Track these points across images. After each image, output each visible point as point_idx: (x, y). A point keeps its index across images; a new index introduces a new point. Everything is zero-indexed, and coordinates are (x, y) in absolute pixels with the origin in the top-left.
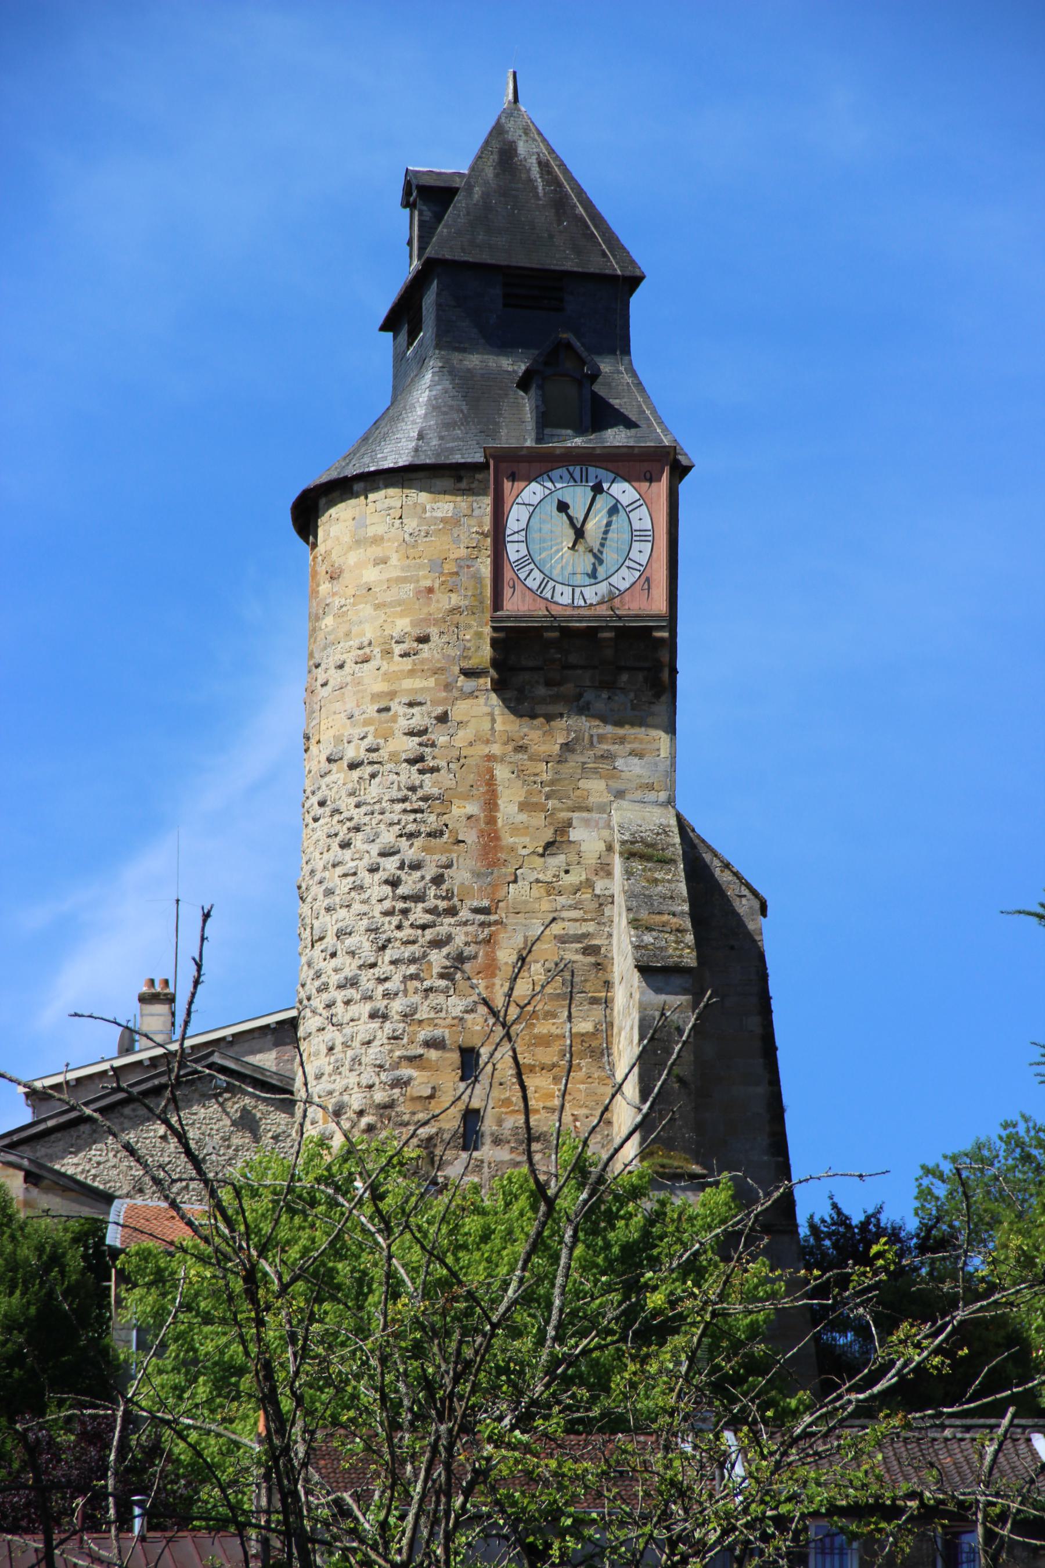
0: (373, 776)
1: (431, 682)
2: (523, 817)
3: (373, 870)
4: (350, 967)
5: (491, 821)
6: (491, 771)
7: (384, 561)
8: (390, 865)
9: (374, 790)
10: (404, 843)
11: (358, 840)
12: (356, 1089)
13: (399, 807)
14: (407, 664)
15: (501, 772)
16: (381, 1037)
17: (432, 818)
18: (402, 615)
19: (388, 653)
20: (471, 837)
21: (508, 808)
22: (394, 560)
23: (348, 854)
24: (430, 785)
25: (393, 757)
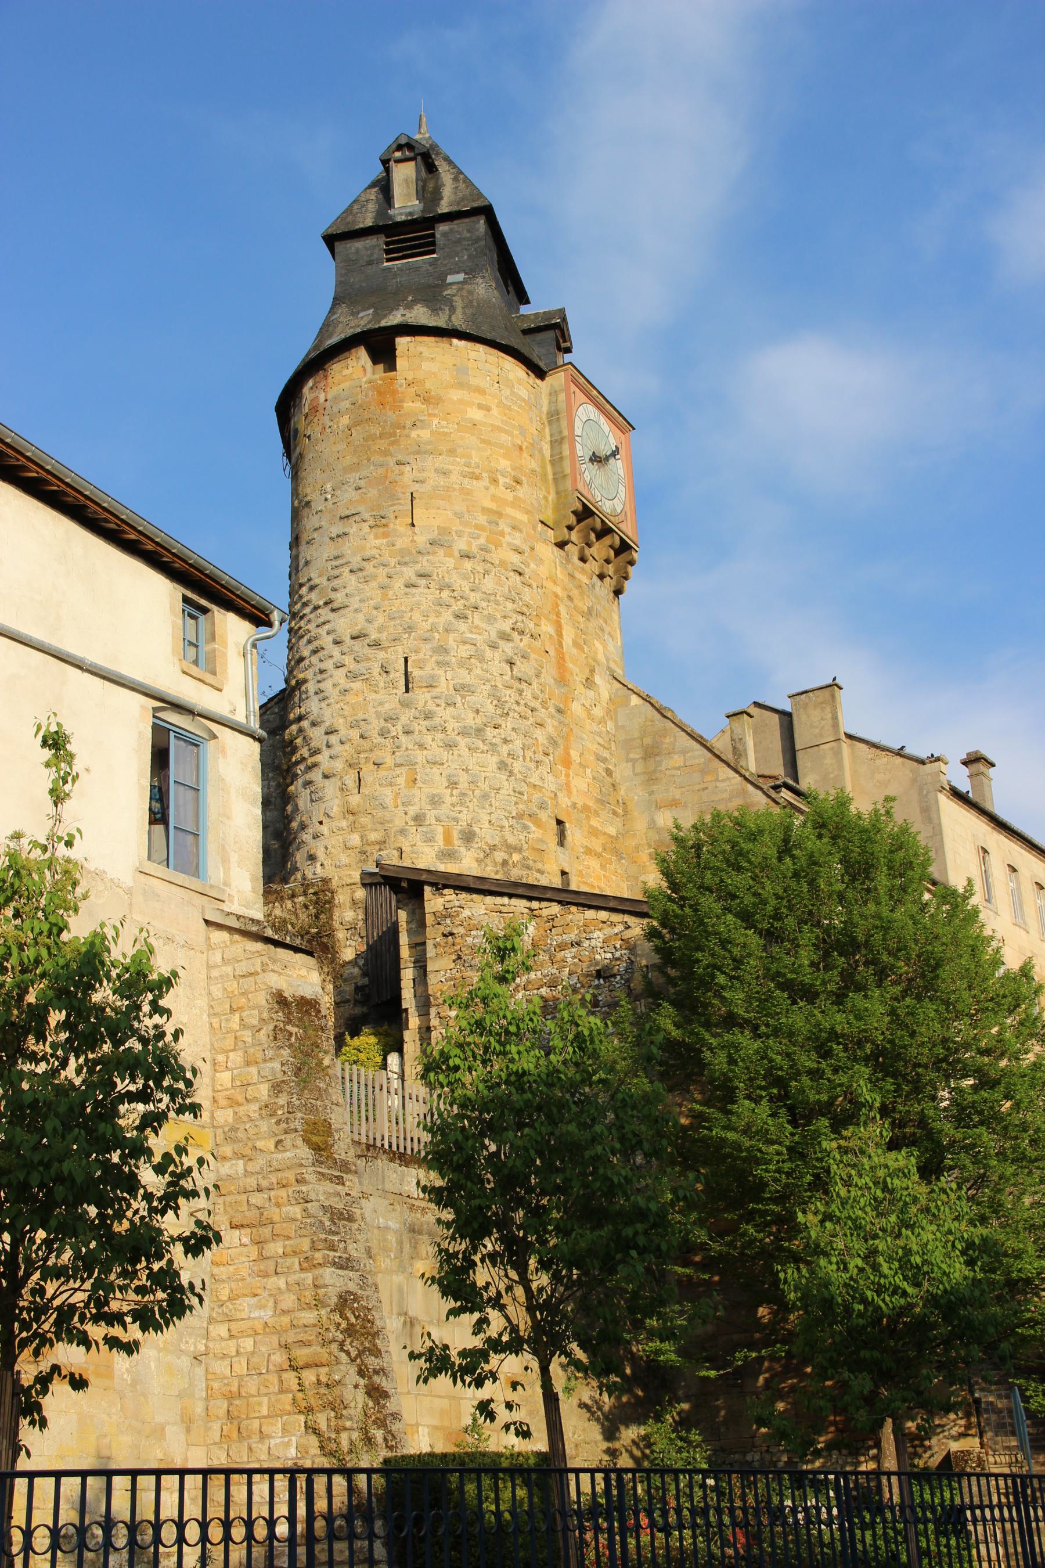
0: (487, 572)
1: (525, 518)
2: (575, 651)
3: (494, 646)
4: (471, 720)
5: (561, 645)
6: (557, 606)
7: (488, 409)
8: (507, 648)
9: (489, 584)
10: (515, 635)
11: (476, 619)
12: (487, 825)
13: (510, 605)
14: (509, 496)
15: (563, 609)
16: (507, 788)
17: (532, 625)
18: (506, 456)
19: (495, 481)
20: (552, 653)
21: (568, 640)
22: (495, 411)
23: (462, 626)
24: (527, 595)
25: (503, 564)
